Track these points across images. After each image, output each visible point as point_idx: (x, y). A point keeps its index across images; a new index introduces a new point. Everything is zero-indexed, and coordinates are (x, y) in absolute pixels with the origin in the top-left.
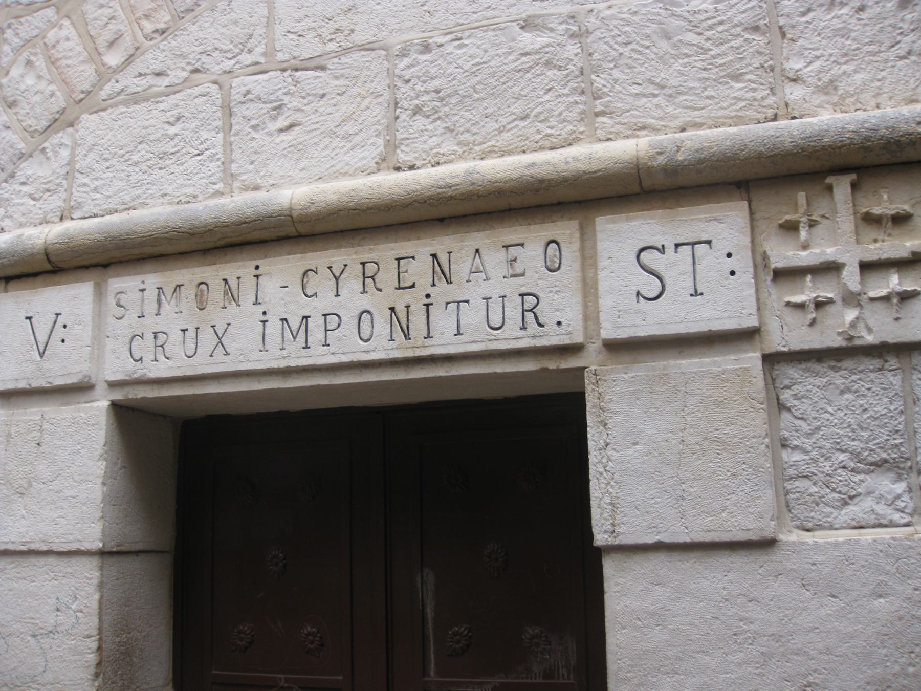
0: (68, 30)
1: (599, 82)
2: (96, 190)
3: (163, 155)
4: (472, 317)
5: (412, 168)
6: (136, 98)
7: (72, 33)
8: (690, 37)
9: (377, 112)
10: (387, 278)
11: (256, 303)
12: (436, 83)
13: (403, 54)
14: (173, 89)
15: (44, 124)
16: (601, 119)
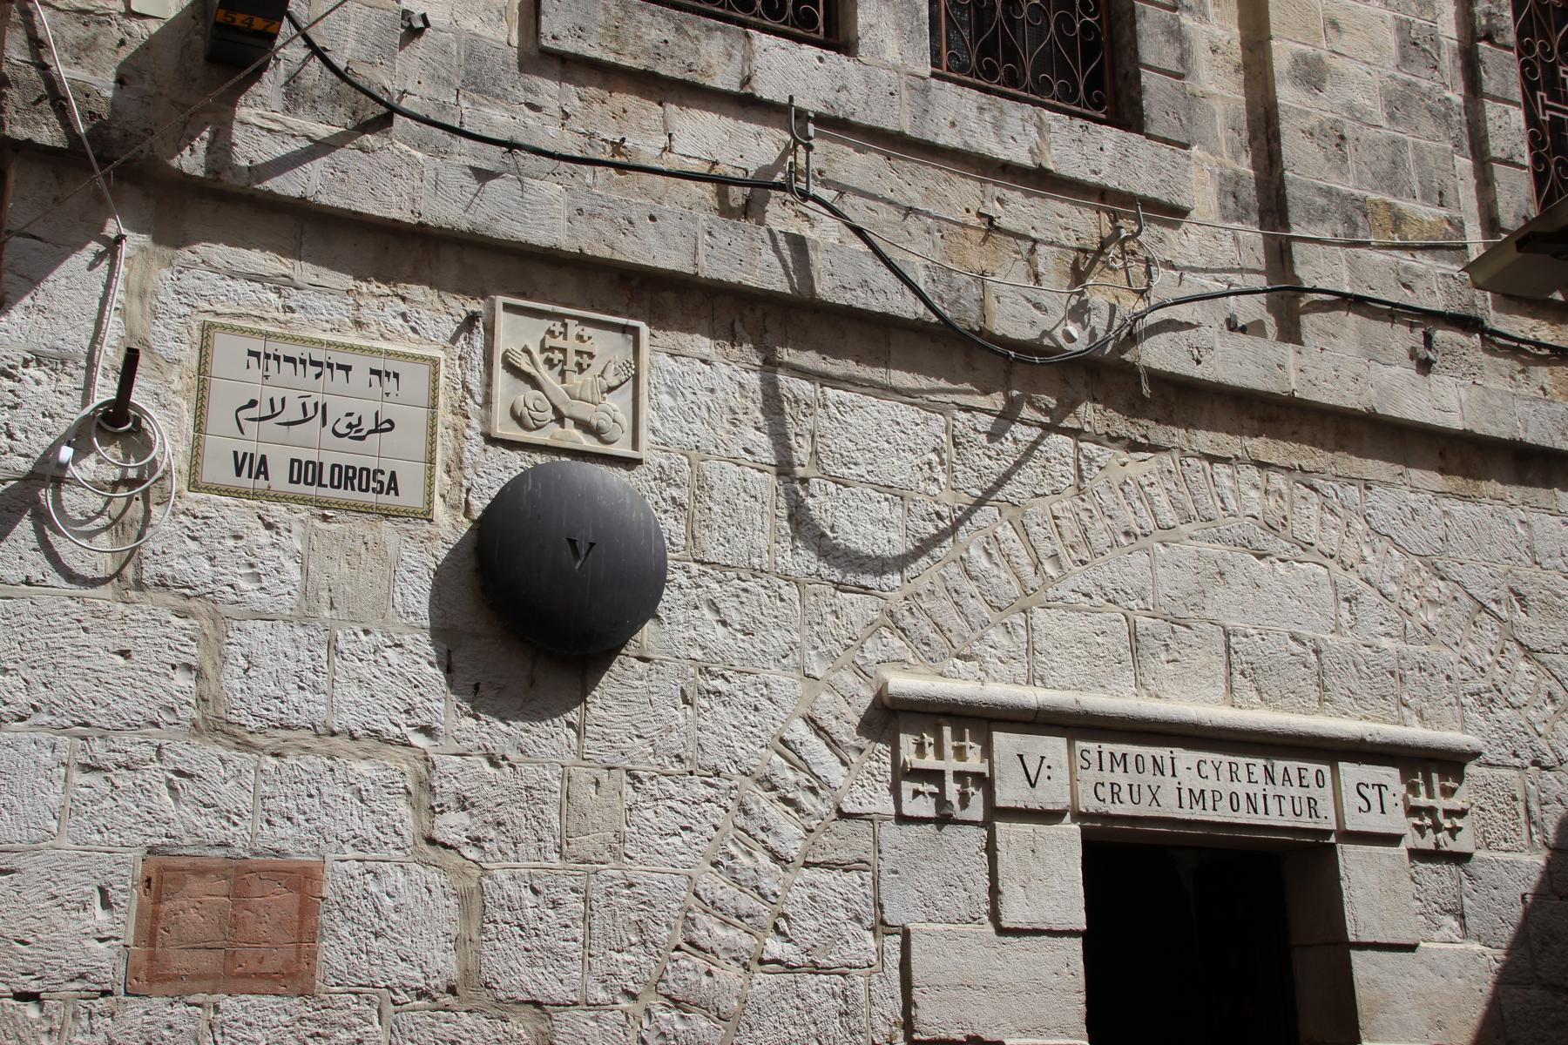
0: (1011, 534)
1: (1327, 682)
4: (1287, 806)
6: (1071, 607)
7: (1016, 537)
8: (1364, 668)
11: (1174, 775)
14: (1096, 610)
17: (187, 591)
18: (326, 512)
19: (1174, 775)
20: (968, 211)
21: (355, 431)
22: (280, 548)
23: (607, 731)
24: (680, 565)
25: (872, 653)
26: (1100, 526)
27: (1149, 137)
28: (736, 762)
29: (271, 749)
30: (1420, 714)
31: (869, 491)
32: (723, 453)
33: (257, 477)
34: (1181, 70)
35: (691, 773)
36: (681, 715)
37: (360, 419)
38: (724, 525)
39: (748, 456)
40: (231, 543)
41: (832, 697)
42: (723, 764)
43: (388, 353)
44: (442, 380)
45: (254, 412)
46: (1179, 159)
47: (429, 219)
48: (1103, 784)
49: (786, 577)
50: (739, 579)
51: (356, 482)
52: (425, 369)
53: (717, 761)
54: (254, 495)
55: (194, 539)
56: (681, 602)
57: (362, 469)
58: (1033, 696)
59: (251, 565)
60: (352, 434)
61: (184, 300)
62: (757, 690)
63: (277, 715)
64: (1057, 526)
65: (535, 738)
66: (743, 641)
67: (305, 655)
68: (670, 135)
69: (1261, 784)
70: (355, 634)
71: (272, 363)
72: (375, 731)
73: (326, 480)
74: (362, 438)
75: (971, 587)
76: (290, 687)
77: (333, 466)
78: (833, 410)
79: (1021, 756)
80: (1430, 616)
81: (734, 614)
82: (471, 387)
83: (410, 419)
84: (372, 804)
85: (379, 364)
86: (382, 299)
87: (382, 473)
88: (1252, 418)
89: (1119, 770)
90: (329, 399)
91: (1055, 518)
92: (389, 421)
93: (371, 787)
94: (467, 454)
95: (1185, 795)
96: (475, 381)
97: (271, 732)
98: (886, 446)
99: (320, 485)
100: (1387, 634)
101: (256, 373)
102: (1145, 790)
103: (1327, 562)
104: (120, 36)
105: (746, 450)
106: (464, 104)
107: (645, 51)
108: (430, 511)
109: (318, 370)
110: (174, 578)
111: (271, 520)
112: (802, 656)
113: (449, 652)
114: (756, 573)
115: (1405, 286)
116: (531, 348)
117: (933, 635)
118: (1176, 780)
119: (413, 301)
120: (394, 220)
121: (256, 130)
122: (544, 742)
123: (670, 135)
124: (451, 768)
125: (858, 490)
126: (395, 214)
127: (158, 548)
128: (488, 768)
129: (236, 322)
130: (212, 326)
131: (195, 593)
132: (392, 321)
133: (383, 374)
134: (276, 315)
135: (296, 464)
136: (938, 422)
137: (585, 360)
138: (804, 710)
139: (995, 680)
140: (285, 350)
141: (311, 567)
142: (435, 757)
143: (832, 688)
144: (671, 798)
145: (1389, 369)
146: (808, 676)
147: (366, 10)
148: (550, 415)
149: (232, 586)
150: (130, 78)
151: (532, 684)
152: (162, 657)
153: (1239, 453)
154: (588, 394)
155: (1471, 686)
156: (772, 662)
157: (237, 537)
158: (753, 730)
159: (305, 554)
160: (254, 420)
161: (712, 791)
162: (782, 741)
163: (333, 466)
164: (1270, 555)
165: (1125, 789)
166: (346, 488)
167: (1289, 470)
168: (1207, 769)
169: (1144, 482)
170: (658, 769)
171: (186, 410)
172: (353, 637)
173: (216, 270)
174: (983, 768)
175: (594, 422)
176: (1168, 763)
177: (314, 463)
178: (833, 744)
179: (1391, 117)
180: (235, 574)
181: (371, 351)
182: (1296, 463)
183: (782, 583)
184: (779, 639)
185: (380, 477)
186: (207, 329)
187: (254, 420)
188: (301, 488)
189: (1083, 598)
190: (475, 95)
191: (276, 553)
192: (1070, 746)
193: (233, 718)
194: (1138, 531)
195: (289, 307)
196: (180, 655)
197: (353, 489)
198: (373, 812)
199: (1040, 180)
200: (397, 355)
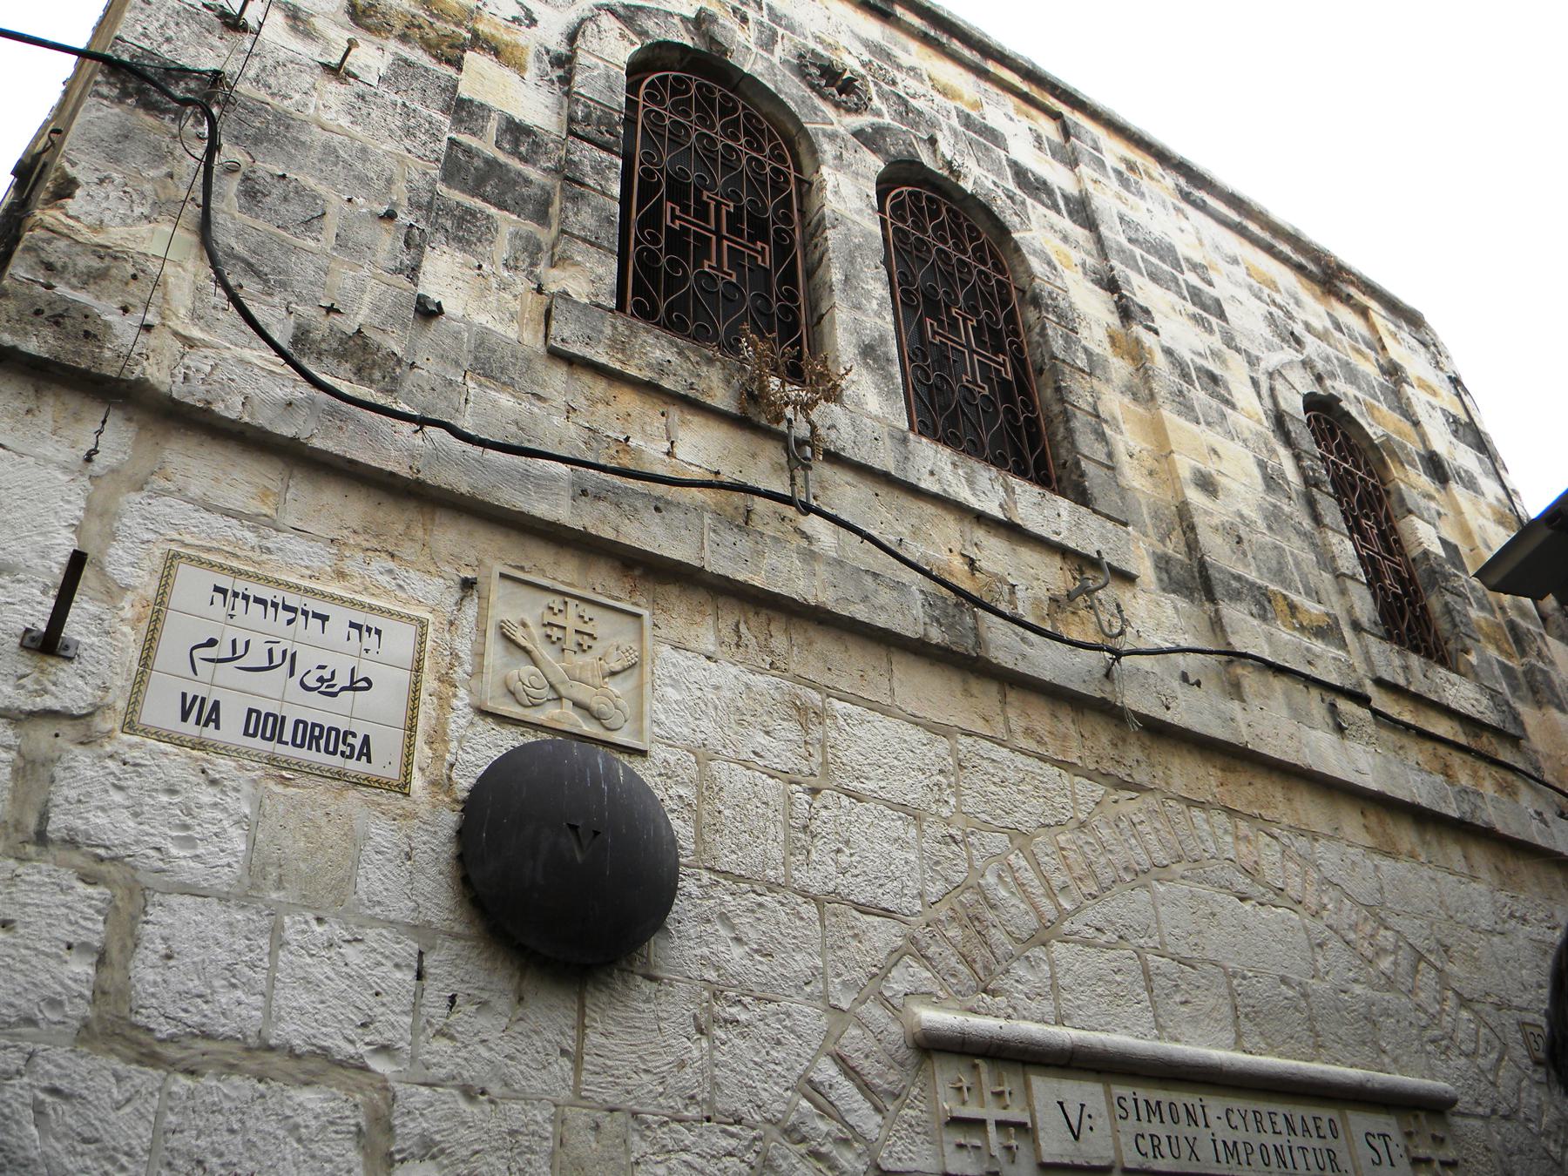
0: (1024, 863)
1: (1318, 1028)
2: (1078, 1007)
3: (1116, 995)
5: (1251, 1053)
6: (1087, 943)
9: (1226, 1010)
10: (1267, 1124)
11: (1207, 1126)
12: (1251, 1002)
13: (1234, 975)
14: (1109, 946)
15: (1025, 936)
16: (1322, 1050)
17: (101, 852)
18: (284, 773)
19: (1207, 1126)
20: (951, 551)
21: (326, 686)
22: (225, 810)
23: (609, 1063)
24: (689, 871)
25: (898, 982)
26: (1103, 860)
27: (1095, 511)
28: (759, 1107)
29: (186, 1064)
30: (1395, 1060)
31: (882, 807)
32: (732, 754)
33: (206, 725)
34: (1110, 464)
35: (708, 1119)
36: (697, 1049)
37: (333, 673)
38: (735, 831)
39: (757, 759)
40: (164, 799)
41: (859, 1032)
42: (745, 1109)
43: (372, 608)
44: (429, 644)
45: (210, 652)
46: (1121, 533)
47: (427, 476)
48: (1143, 1136)
49: (804, 893)
50: (754, 892)
51: (322, 743)
52: (410, 631)
53: (738, 1105)
54: (200, 745)
55: (120, 788)
56: (692, 914)
57: (330, 729)
58: (1066, 1035)
59: (186, 827)
60: (322, 689)
61: (151, 527)
62: (780, 1021)
63: (197, 1019)
64: (1064, 857)
65: (523, 1068)
66: (761, 963)
67: (241, 944)
68: (672, 443)
69: (1285, 1136)
70: (306, 922)
71: (240, 602)
72: (322, 1048)
73: (287, 736)
74: (334, 695)
75: (990, 915)
76: (217, 983)
77: (297, 722)
78: (841, 721)
79: (1061, 1104)
80: (1385, 964)
81: (747, 929)
82: (461, 654)
83: (390, 685)
84: (314, 1146)
85: (359, 618)
86: (370, 553)
87: (354, 735)
88: (1214, 767)
89: (1156, 1119)
90: (297, 647)
91: (1062, 849)
92: (366, 680)
93: (313, 1122)
94: (453, 726)
95: (1220, 1147)
96: (464, 647)
97: (186, 1041)
98: (896, 763)
99: (280, 741)
100: (1355, 981)
101: (219, 610)
102: (1183, 1142)
103: (1298, 908)
104: (132, 271)
105: (755, 753)
106: (471, 384)
107: (649, 365)
108: (407, 784)
109: (291, 615)
110: (89, 837)
111: (217, 776)
112: (826, 984)
113: (421, 954)
114: (772, 887)
115: (1309, 662)
116: (529, 622)
117: (960, 967)
118: (1210, 1131)
119: (401, 559)
120: (392, 474)
121: (256, 370)
122: (533, 1073)
123: (672, 443)
124: (416, 1102)
125: (871, 805)
126: (390, 467)
127: (73, 794)
128: (463, 1105)
129: (205, 556)
130: (177, 556)
131: (112, 854)
132: (379, 577)
133: (364, 629)
134: (250, 554)
135: (254, 715)
136: (942, 746)
137: (587, 641)
138: (831, 1047)
139: (1025, 1018)
140: (255, 590)
141: (260, 836)
142: (399, 1088)
143: (862, 1024)
144: (685, 1150)
145: (1314, 732)
146: (834, 1007)
147: (384, 287)
148: (546, 693)
149: (158, 849)
150: (135, 306)
151: (521, 1000)
152: (57, 933)
153: (1210, 798)
154: (587, 675)
155: (1429, 1033)
156: (793, 990)
157: (172, 791)
158: (779, 1069)
159: (253, 819)
160: (212, 660)
161: (734, 1142)
162: (810, 1082)
163: (297, 722)
164: (1250, 898)
165: (1164, 1141)
166: (310, 748)
167: (1252, 817)
168: (1236, 1119)
169: (1136, 820)
170: (670, 1112)
171: (130, 640)
172: (304, 926)
173: (191, 501)
174: (1024, 1117)
175: (594, 706)
176: (1199, 1111)
177: (275, 717)
178: (866, 1088)
179: (1270, 528)
180: (165, 836)
181: (353, 603)
182: (1256, 811)
183: (800, 900)
184: (802, 963)
185: (350, 739)
186: (172, 559)
187: (212, 660)
188: (257, 743)
189: (1096, 933)
190: (482, 379)
191: (220, 816)
192: (1108, 1095)
193: (140, 1019)
194: (1137, 868)
195: (268, 549)
196: (81, 932)
197: (318, 750)
198: (313, 1157)
199: (1012, 531)
200: (381, 611)
